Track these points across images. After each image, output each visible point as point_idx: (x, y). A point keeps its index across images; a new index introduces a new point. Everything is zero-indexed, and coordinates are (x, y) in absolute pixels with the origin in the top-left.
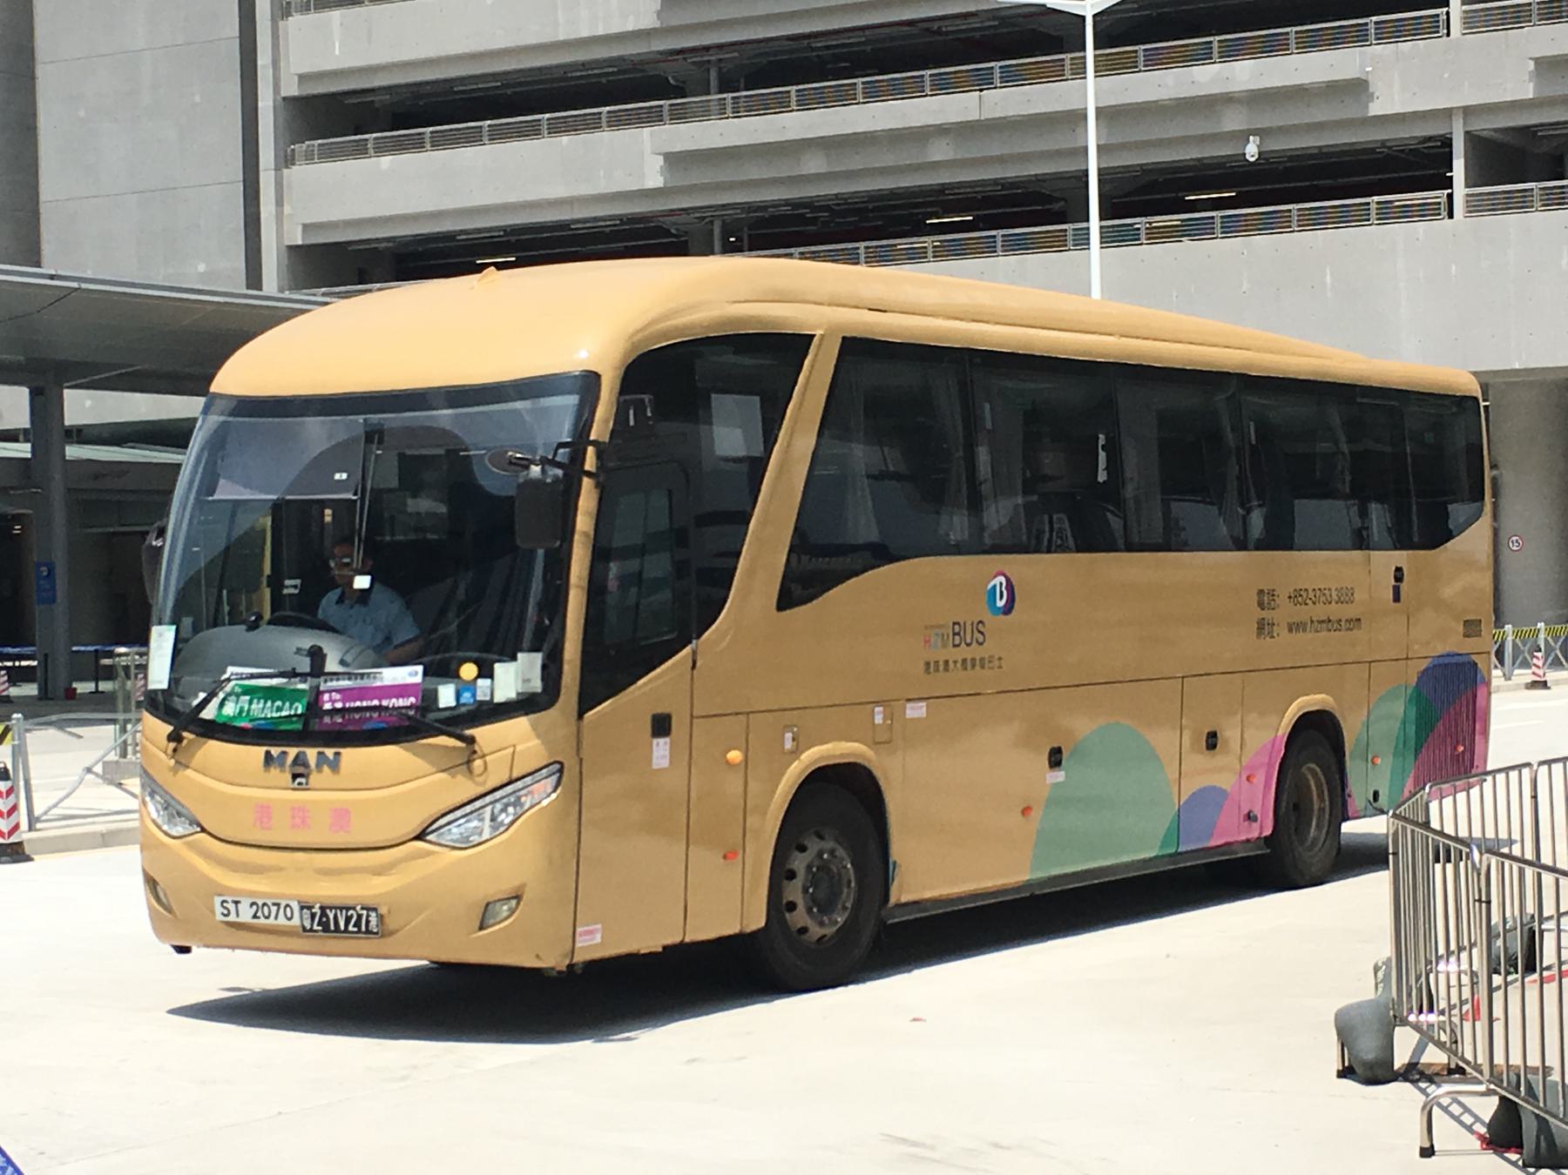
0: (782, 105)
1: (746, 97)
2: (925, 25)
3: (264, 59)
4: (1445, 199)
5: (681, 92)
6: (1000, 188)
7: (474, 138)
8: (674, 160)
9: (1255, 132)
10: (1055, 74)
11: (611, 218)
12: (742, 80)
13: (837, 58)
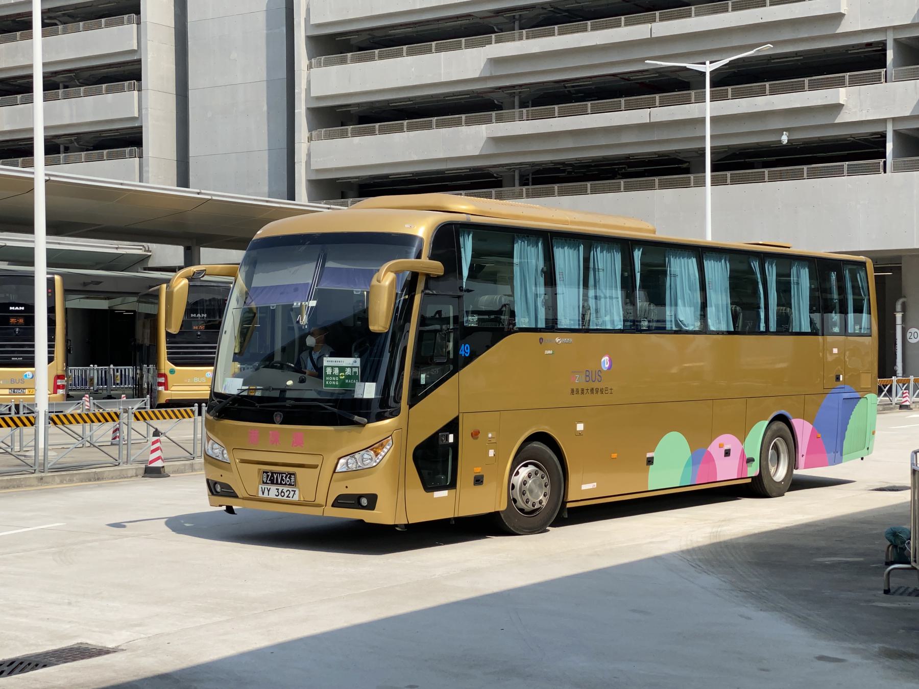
2: (621, 76)
4: (882, 164)
5: (499, 108)
6: (657, 156)
7: (400, 130)
8: (497, 140)
9: (787, 130)
10: (687, 101)
11: (466, 168)
12: (530, 102)
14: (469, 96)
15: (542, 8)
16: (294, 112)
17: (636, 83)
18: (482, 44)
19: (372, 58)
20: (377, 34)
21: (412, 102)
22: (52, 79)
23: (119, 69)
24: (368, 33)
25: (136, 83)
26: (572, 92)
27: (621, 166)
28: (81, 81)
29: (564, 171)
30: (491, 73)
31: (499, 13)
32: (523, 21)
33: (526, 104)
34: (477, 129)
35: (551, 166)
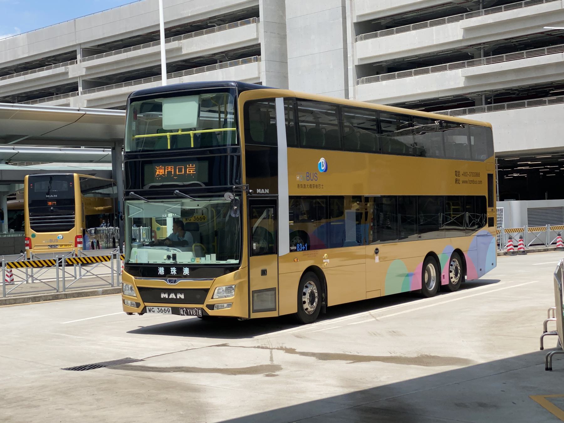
0: (501, 60)
1: (492, 58)
3: (349, 55)
5: (473, 58)
7: (410, 75)
8: (469, 78)
11: (451, 96)
12: (491, 52)
13: (520, 44)
16: (348, 68)
17: (557, 36)
18: (457, 20)
19: (392, 33)
20: (396, 18)
22: (214, 57)
23: (249, 49)
26: (516, 45)
27: (550, 89)
28: (229, 57)
29: (514, 94)
32: (485, 3)
34: (456, 72)
35: (504, 91)
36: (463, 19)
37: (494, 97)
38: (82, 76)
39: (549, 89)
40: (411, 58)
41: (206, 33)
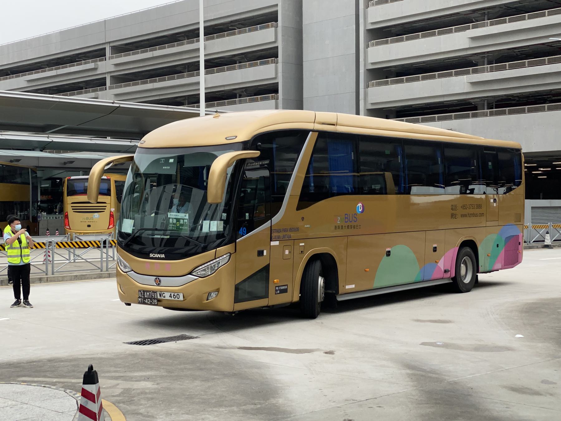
0: (504, 68)
2: (547, 44)
5: (476, 65)
7: (417, 79)
8: (473, 84)
12: (494, 61)
13: (522, 54)
14: (457, 59)
15: (500, 7)
17: (558, 48)
20: (406, 26)
21: (425, 64)
22: (234, 58)
24: (401, 26)
25: (275, 59)
27: (548, 96)
28: (248, 59)
29: (514, 100)
30: (470, 46)
31: (476, 11)
33: (491, 62)
35: (504, 97)
36: (469, 29)
37: (495, 103)
38: (110, 72)
39: (547, 96)
40: (419, 64)
41: (228, 35)
